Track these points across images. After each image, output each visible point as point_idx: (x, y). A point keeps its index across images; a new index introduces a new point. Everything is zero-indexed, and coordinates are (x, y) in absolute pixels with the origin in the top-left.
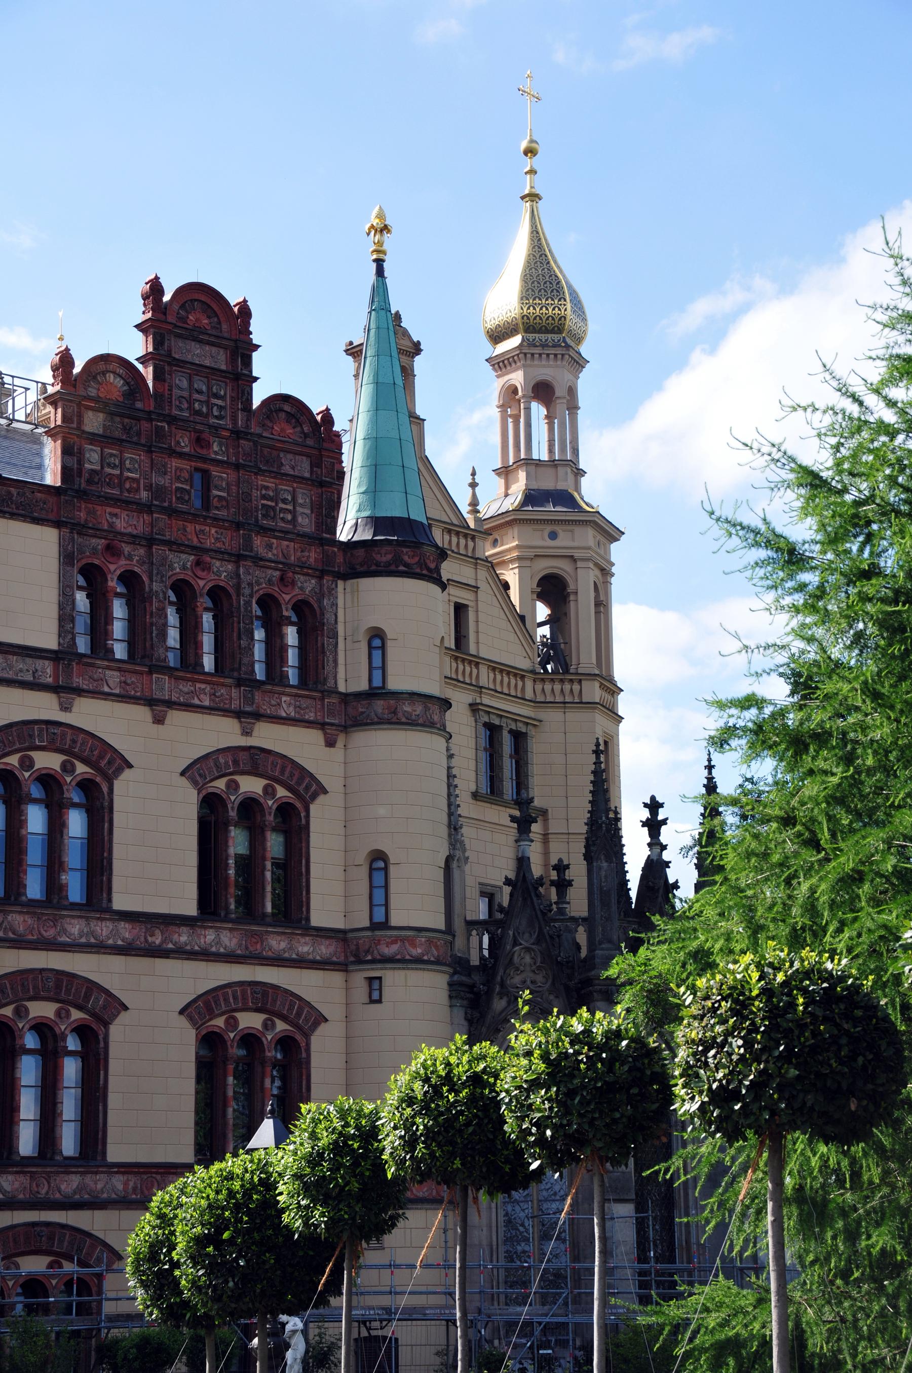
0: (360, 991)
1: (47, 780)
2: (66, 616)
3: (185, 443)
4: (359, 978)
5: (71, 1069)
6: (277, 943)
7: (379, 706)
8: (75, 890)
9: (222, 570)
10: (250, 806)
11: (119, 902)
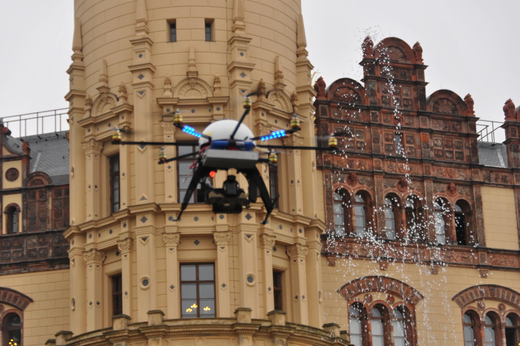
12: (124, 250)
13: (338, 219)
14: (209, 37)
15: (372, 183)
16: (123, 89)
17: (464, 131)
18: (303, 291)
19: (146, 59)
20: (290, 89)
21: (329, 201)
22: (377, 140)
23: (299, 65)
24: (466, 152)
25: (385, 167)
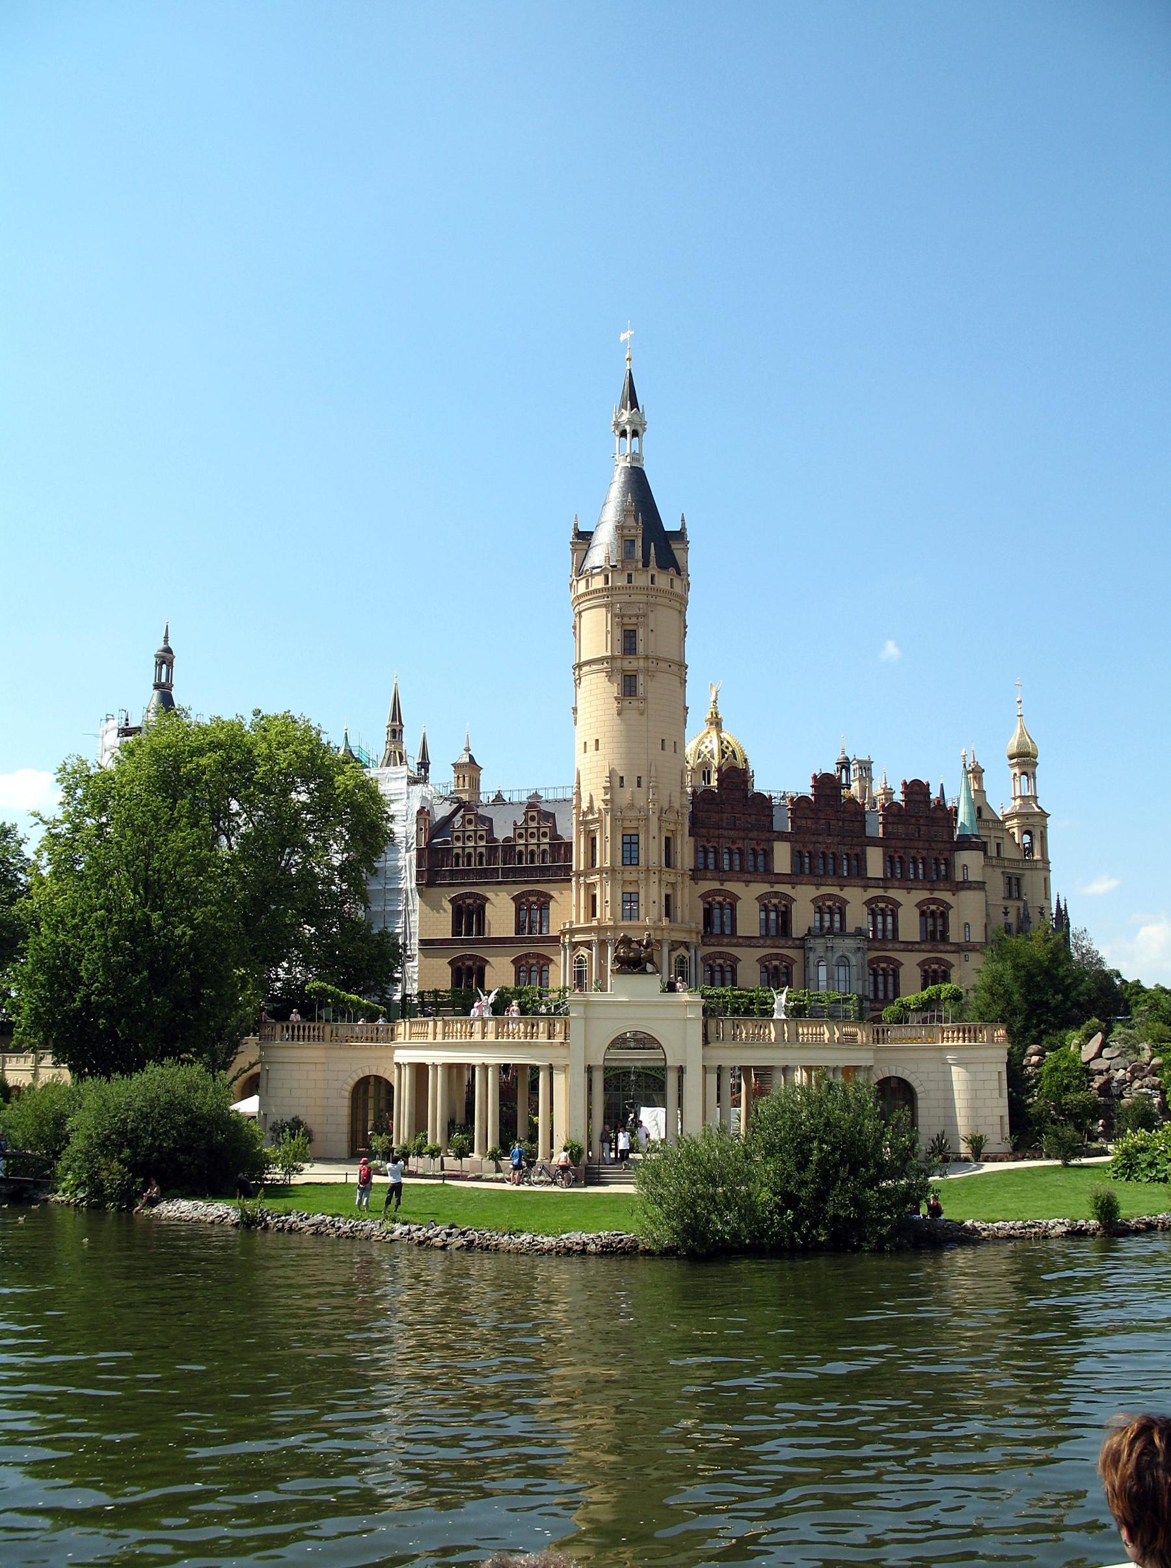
0: (963, 959)
1: (882, 909)
2: (885, 870)
3: (913, 821)
4: (962, 955)
5: (890, 979)
6: (941, 947)
7: (966, 885)
8: (890, 935)
9: (924, 853)
10: (933, 912)
11: (900, 939)
12: (598, 887)
13: (701, 860)
14: (639, 786)
15: (718, 843)
16: (600, 810)
17: (767, 813)
18: (679, 905)
19: (608, 797)
20: (676, 806)
21: (696, 851)
22: (722, 820)
23: (682, 793)
24: (767, 824)
25: (725, 833)
